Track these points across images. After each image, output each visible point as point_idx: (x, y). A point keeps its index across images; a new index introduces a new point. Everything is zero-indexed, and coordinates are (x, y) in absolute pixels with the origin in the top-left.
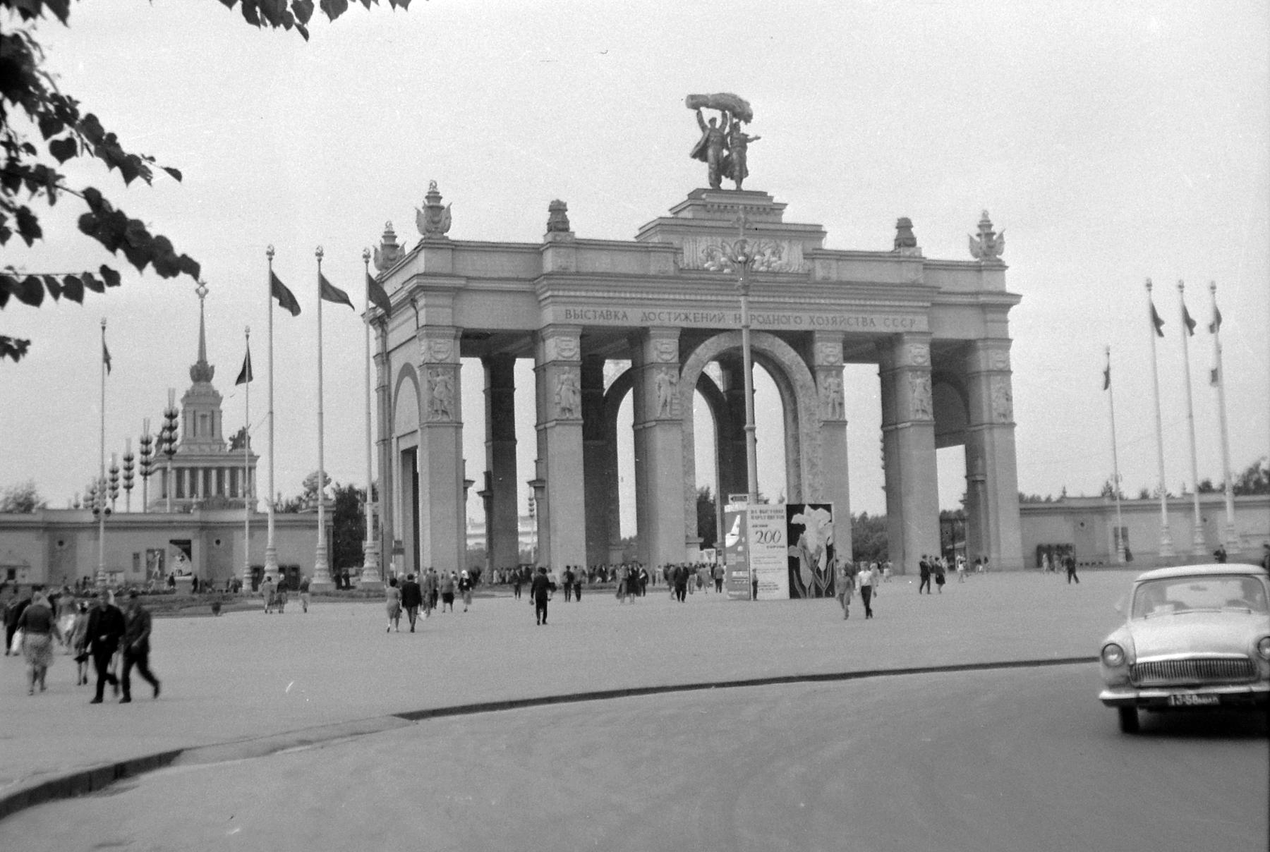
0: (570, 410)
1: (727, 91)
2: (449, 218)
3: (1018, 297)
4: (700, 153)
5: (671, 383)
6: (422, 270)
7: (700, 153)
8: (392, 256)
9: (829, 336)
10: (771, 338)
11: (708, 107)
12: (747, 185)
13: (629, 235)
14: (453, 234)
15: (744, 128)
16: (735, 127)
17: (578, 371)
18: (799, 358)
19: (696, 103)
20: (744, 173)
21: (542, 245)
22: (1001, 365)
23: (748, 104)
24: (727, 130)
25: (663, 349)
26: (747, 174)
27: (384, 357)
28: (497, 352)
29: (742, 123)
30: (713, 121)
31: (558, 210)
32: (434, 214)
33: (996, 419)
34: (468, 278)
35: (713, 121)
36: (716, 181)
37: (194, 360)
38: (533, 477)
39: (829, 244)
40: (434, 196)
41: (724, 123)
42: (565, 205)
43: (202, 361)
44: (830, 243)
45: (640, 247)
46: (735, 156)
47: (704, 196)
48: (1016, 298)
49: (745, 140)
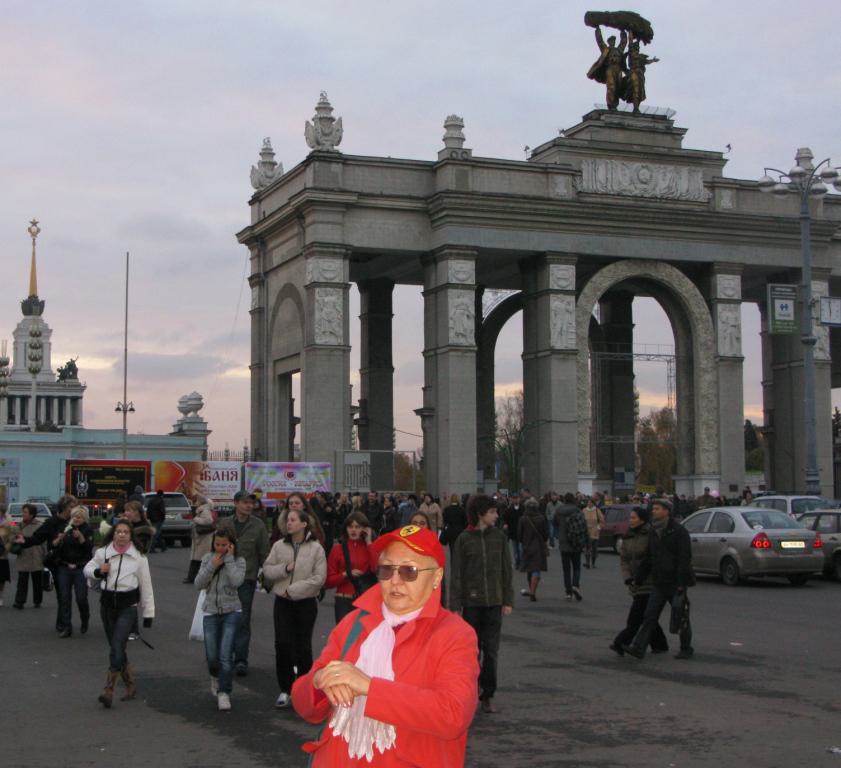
0: (464, 336)
1: (627, 9)
2: (340, 130)
4: (598, 73)
5: (567, 311)
6: (310, 184)
7: (598, 73)
8: (270, 174)
9: (729, 268)
10: (669, 269)
11: (607, 24)
12: (645, 106)
13: (522, 157)
14: (346, 148)
15: (644, 49)
16: (635, 47)
18: (698, 292)
19: (594, 19)
20: (642, 96)
21: (437, 163)
23: (649, 23)
24: (626, 50)
25: (562, 275)
26: (644, 97)
27: (258, 280)
28: (376, 275)
29: (641, 43)
30: (612, 40)
31: (454, 125)
32: (325, 123)
34: (361, 195)
36: (612, 102)
37: (25, 296)
38: (420, 405)
39: (729, 172)
40: (324, 107)
41: (623, 43)
44: (729, 172)
45: (539, 163)
46: (634, 77)
47: (603, 117)
49: (643, 61)
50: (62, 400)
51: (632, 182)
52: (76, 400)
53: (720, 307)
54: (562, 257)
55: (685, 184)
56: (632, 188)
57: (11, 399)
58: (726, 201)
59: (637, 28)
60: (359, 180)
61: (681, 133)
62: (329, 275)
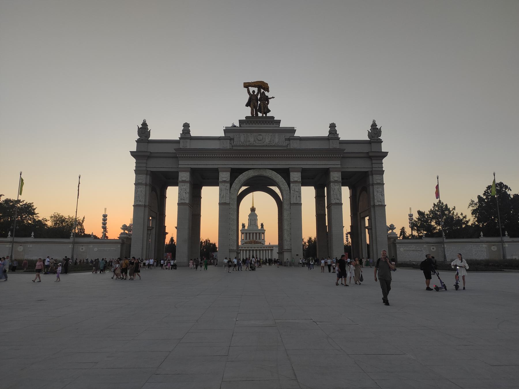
3: (387, 153)
9: (295, 170)
12: (268, 115)
14: (151, 138)
15: (266, 93)
17: (188, 184)
19: (247, 85)
22: (379, 181)
25: (224, 176)
30: (254, 92)
31: (186, 126)
35: (254, 92)
39: (296, 134)
40: (145, 125)
48: (385, 154)
49: (267, 99)
50: (259, 233)
52: (264, 233)
53: (291, 185)
54: (225, 170)
55: (278, 140)
58: (295, 145)
59: (263, 86)
60: (153, 149)
61: (279, 122)
62: (140, 181)
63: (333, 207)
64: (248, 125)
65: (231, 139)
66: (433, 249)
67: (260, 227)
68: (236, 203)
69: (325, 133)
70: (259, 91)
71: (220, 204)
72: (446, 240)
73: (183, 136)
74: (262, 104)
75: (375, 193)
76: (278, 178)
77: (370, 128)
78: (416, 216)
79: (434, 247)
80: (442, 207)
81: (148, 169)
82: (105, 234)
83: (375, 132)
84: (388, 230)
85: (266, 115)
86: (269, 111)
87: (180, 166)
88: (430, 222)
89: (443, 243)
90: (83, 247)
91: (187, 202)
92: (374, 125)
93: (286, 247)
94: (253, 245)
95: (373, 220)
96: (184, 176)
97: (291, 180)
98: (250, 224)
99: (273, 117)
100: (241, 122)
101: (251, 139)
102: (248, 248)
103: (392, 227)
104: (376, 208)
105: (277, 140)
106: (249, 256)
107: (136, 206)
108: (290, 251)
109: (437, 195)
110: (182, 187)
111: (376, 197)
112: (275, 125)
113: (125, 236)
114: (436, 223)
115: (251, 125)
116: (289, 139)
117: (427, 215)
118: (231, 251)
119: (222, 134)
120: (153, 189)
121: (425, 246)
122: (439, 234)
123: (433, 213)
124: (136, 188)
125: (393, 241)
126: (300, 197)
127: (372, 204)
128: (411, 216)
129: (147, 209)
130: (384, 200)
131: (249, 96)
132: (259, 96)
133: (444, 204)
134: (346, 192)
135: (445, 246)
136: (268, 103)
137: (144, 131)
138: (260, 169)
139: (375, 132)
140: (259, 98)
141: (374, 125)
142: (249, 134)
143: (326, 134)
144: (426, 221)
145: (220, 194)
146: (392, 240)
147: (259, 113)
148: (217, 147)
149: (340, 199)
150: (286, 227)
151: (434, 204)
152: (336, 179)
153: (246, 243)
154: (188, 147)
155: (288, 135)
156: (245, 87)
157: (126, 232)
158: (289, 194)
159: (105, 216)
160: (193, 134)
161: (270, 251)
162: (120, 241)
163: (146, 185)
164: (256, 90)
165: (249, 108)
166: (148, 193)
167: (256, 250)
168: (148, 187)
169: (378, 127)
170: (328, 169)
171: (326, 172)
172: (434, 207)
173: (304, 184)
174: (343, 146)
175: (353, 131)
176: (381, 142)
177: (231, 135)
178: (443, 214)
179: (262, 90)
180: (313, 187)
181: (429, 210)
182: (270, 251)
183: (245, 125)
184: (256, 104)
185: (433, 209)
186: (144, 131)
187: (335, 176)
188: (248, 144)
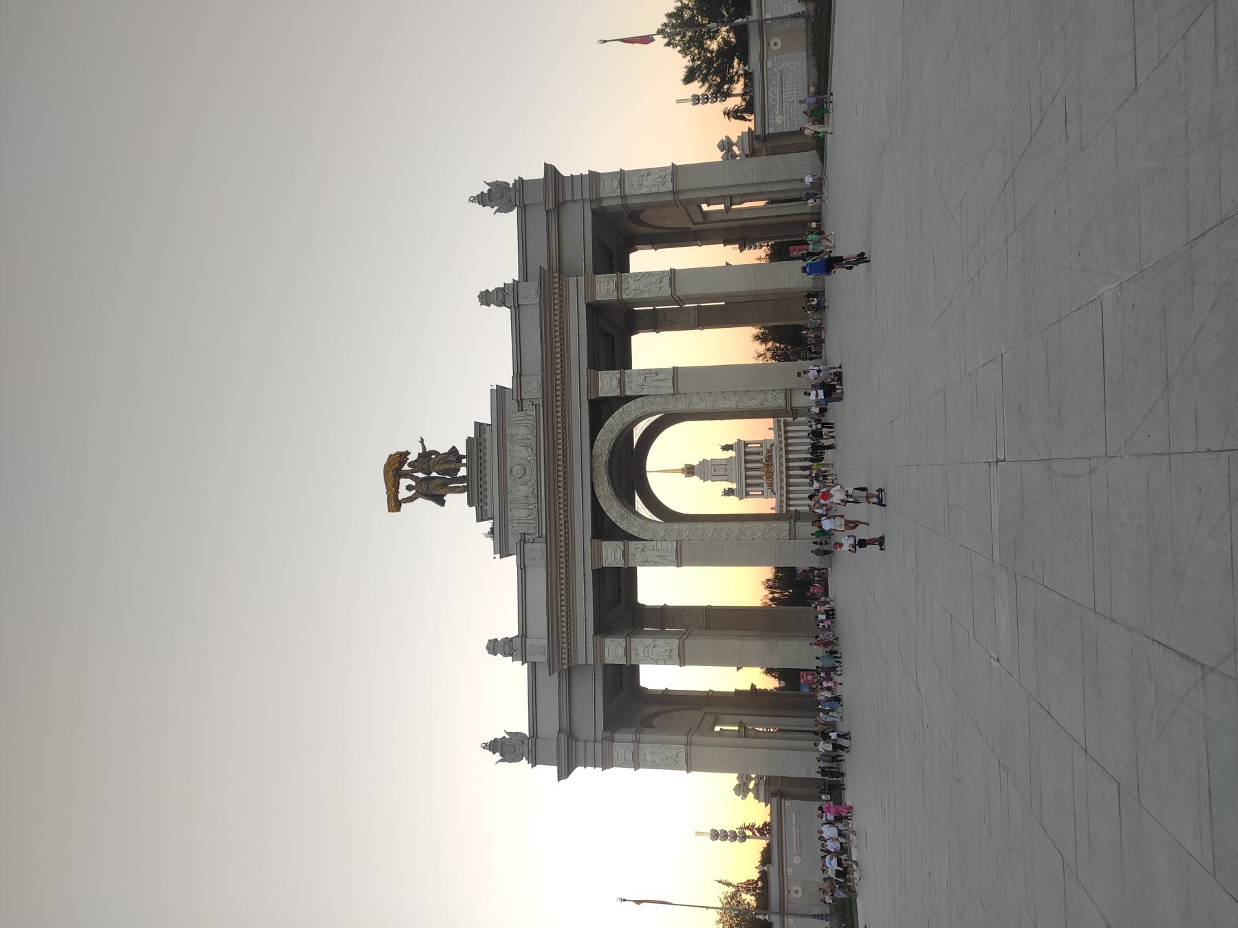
9: (593, 384)
12: (462, 451)
14: (524, 728)
15: (413, 457)
19: (395, 504)
22: (616, 183)
25: (612, 554)
30: (409, 488)
31: (494, 647)
33: (669, 186)
35: (409, 488)
40: (493, 746)
42: (490, 641)
43: (683, 471)
48: (550, 170)
49: (426, 455)
50: (746, 454)
51: (526, 484)
52: (746, 444)
53: (629, 393)
54: (597, 554)
55: (522, 428)
56: (530, 484)
57: (747, 485)
58: (533, 389)
59: (395, 467)
60: (550, 725)
61: (479, 427)
62: (629, 756)
63: (681, 292)
64: (489, 500)
65: (523, 540)
66: (775, 44)
67: (732, 454)
68: (675, 526)
69: (503, 315)
70: (407, 475)
71: (679, 563)
72: (754, 16)
73: (519, 654)
74: (437, 468)
75: (646, 191)
76: (613, 425)
77: (488, 208)
78: (697, 88)
79: (772, 43)
80: (674, 26)
81: (600, 736)
82: (758, 829)
83: (498, 196)
84: (734, 156)
85: (463, 457)
86: (454, 450)
87: (591, 662)
88: (712, 52)
89: (761, 23)
90: (793, 889)
91: (675, 642)
92: (482, 199)
93: (780, 402)
94: (776, 468)
95: (709, 194)
96: (614, 651)
97: (617, 393)
98: (725, 477)
99: (469, 440)
100: (481, 517)
101: (522, 491)
102: (782, 481)
103: (726, 145)
104: (681, 187)
105: (523, 431)
106: (801, 477)
107: (689, 765)
108: (788, 393)
109: (646, 40)
110: (641, 655)
111: (654, 190)
112: (487, 436)
113: (762, 788)
114: (712, 38)
115: (489, 493)
116: (520, 402)
117: (693, 60)
118: (793, 536)
119: (512, 560)
120: (647, 723)
121: (769, 64)
122: (741, 32)
123: (689, 48)
124: (644, 767)
125: (759, 143)
126: (657, 372)
127: (669, 198)
128: (696, 100)
129: (695, 739)
130: (660, 169)
131: (420, 500)
132: (420, 475)
133: (666, 20)
134: (643, 261)
135: (768, 16)
136: (436, 453)
137: (507, 748)
138: (592, 469)
139: (498, 196)
140: (423, 476)
141: (482, 199)
142: (510, 498)
143: (503, 315)
144: (709, 62)
145: (656, 564)
146: (756, 144)
147: (459, 474)
148: (542, 572)
149: (662, 274)
150: (731, 404)
151: (668, 44)
152: (612, 286)
153: (771, 486)
154: (545, 642)
155: (511, 404)
156: (398, 509)
157: (751, 785)
158: (650, 398)
159: (715, 835)
160: (512, 630)
161: (789, 428)
162: (775, 800)
163: (637, 742)
164: (404, 482)
165: (449, 498)
166: (657, 737)
167: (787, 460)
168: (643, 737)
169: (486, 189)
170: (588, 306)
171: (596, 310)
172: (675, 46)
173: (626, 362)
174: (534, 271)
175: (497, 249)
176: (520, 182)
177: (513, 540)
178: (690, 24)
179: (406, 467)
180: (634, 339)
181: (680, 56)
182: (789, 428)
183: (488, 508)
184: (437, 482)
185: (679, 48)
186: (507, 748)
187: (605, 287)
188: (533, 500)
